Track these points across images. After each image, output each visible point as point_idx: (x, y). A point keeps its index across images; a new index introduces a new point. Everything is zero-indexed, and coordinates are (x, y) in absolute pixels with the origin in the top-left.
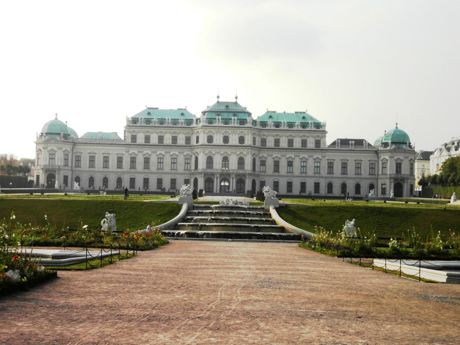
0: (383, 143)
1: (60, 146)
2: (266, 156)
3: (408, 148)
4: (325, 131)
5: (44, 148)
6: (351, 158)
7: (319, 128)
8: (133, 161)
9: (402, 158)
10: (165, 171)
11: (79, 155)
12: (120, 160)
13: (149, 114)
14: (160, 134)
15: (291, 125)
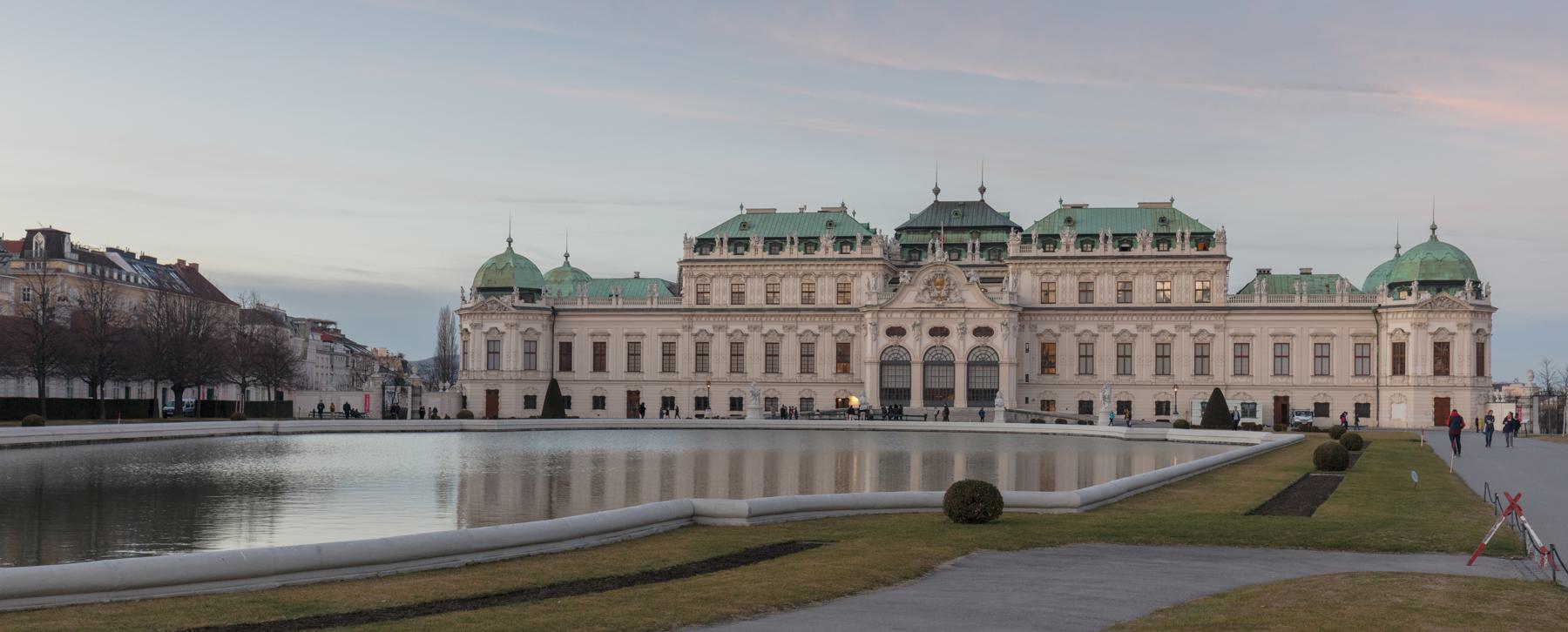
0: (1391, 286)
1: (512, 320)
2: (1056, 330)
3: (1472, 299)
4: (1224, 256)
5: (474, 326)
6: (1302, 333)
7: (1205, 249)
8: (702, 353)
9: (1451, 326)
10: (785, 377)
11: (565, 339)
12: (668, 353)
13: (744, 226)
14: (770, 280)
15: (1124, 241)
